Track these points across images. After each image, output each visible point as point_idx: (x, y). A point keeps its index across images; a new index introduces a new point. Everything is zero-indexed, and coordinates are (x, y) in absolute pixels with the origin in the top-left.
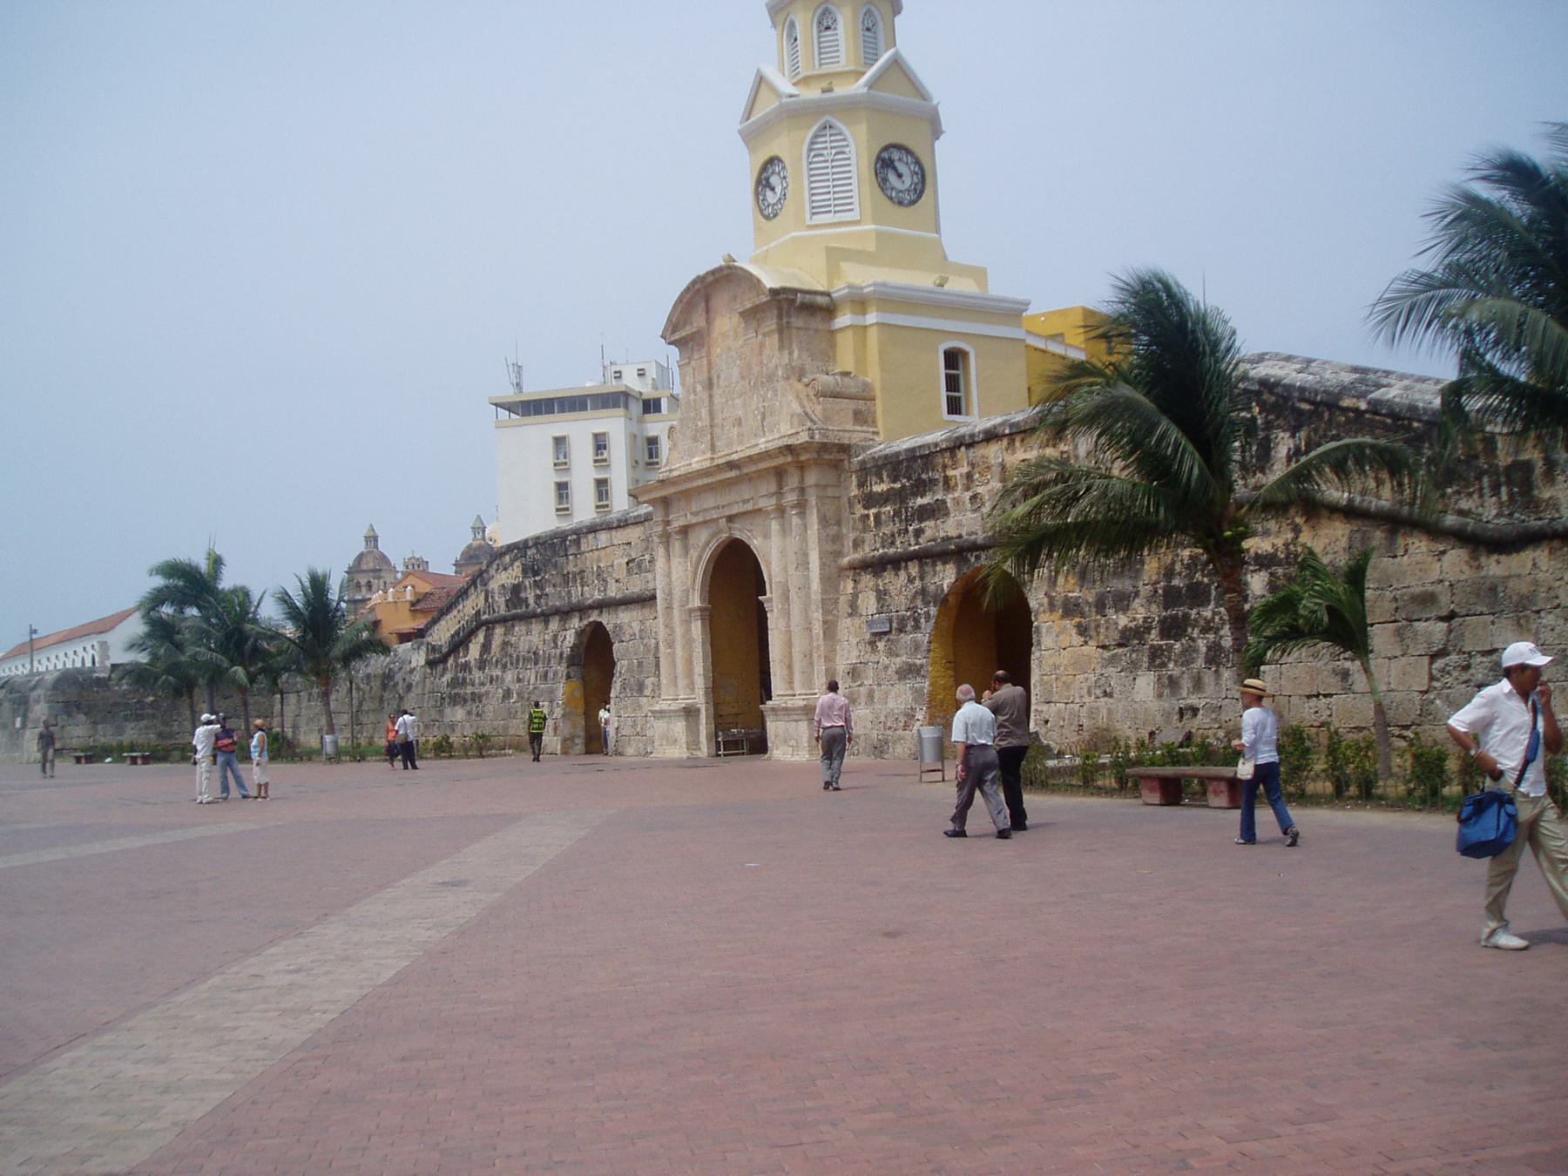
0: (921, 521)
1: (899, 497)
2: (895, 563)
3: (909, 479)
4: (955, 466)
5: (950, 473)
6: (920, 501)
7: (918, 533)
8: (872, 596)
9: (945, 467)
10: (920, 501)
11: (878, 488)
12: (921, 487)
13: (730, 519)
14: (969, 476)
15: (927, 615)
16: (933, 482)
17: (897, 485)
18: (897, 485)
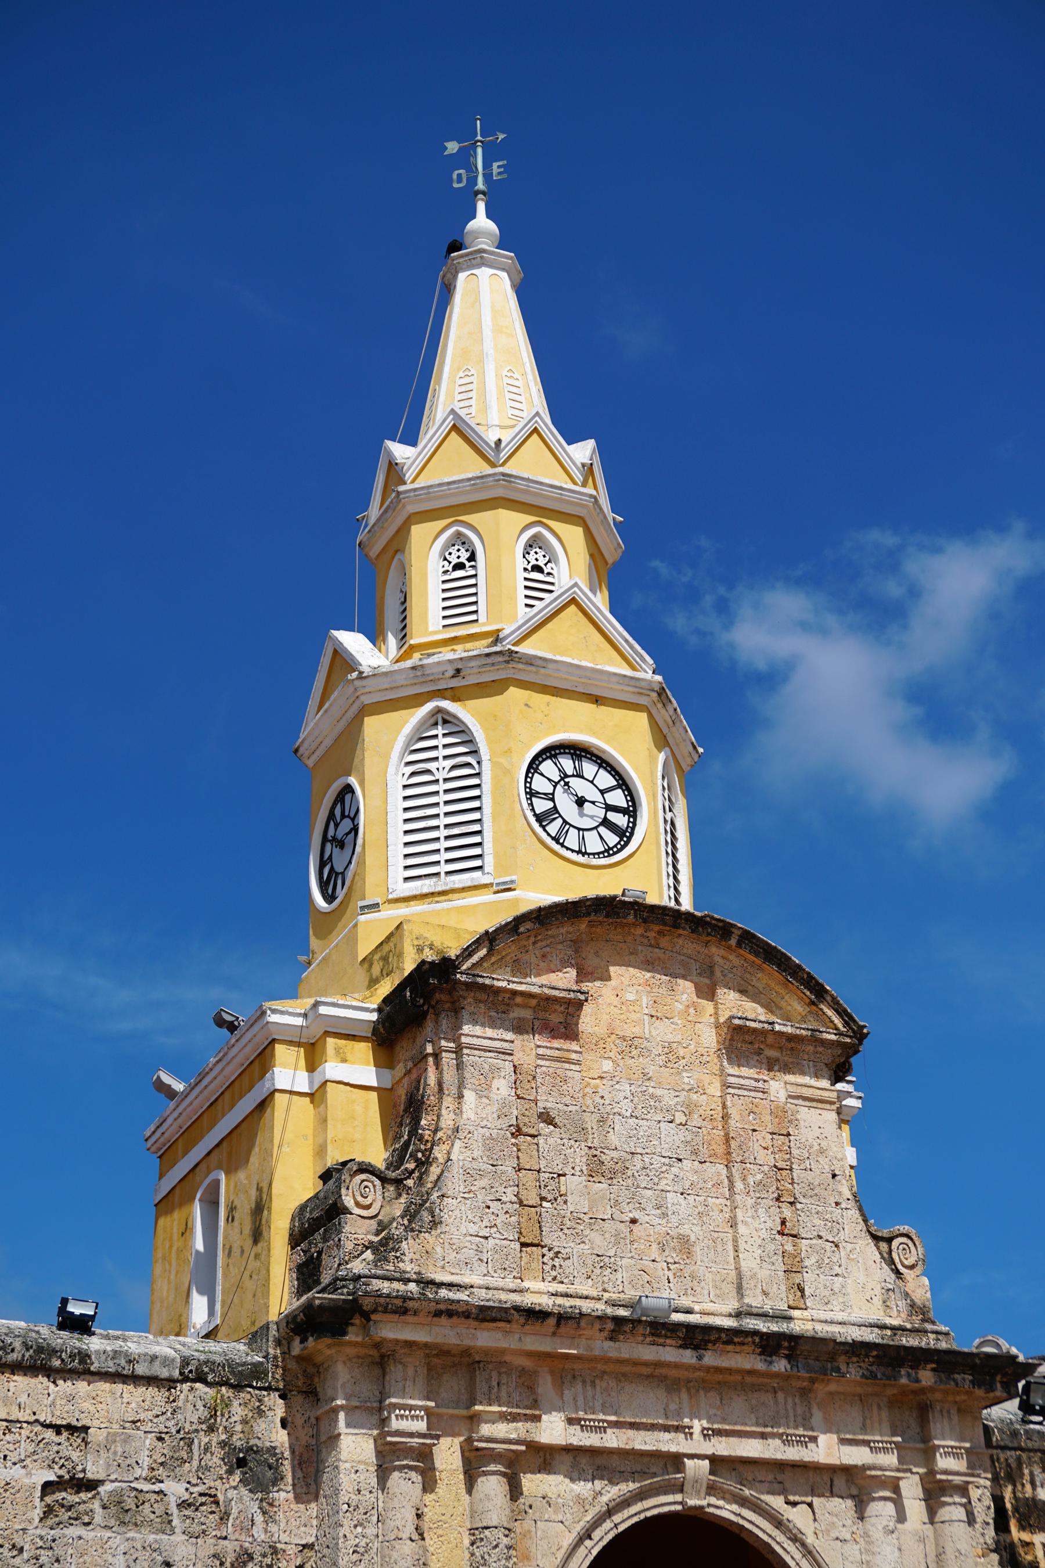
13: (717, 1462)
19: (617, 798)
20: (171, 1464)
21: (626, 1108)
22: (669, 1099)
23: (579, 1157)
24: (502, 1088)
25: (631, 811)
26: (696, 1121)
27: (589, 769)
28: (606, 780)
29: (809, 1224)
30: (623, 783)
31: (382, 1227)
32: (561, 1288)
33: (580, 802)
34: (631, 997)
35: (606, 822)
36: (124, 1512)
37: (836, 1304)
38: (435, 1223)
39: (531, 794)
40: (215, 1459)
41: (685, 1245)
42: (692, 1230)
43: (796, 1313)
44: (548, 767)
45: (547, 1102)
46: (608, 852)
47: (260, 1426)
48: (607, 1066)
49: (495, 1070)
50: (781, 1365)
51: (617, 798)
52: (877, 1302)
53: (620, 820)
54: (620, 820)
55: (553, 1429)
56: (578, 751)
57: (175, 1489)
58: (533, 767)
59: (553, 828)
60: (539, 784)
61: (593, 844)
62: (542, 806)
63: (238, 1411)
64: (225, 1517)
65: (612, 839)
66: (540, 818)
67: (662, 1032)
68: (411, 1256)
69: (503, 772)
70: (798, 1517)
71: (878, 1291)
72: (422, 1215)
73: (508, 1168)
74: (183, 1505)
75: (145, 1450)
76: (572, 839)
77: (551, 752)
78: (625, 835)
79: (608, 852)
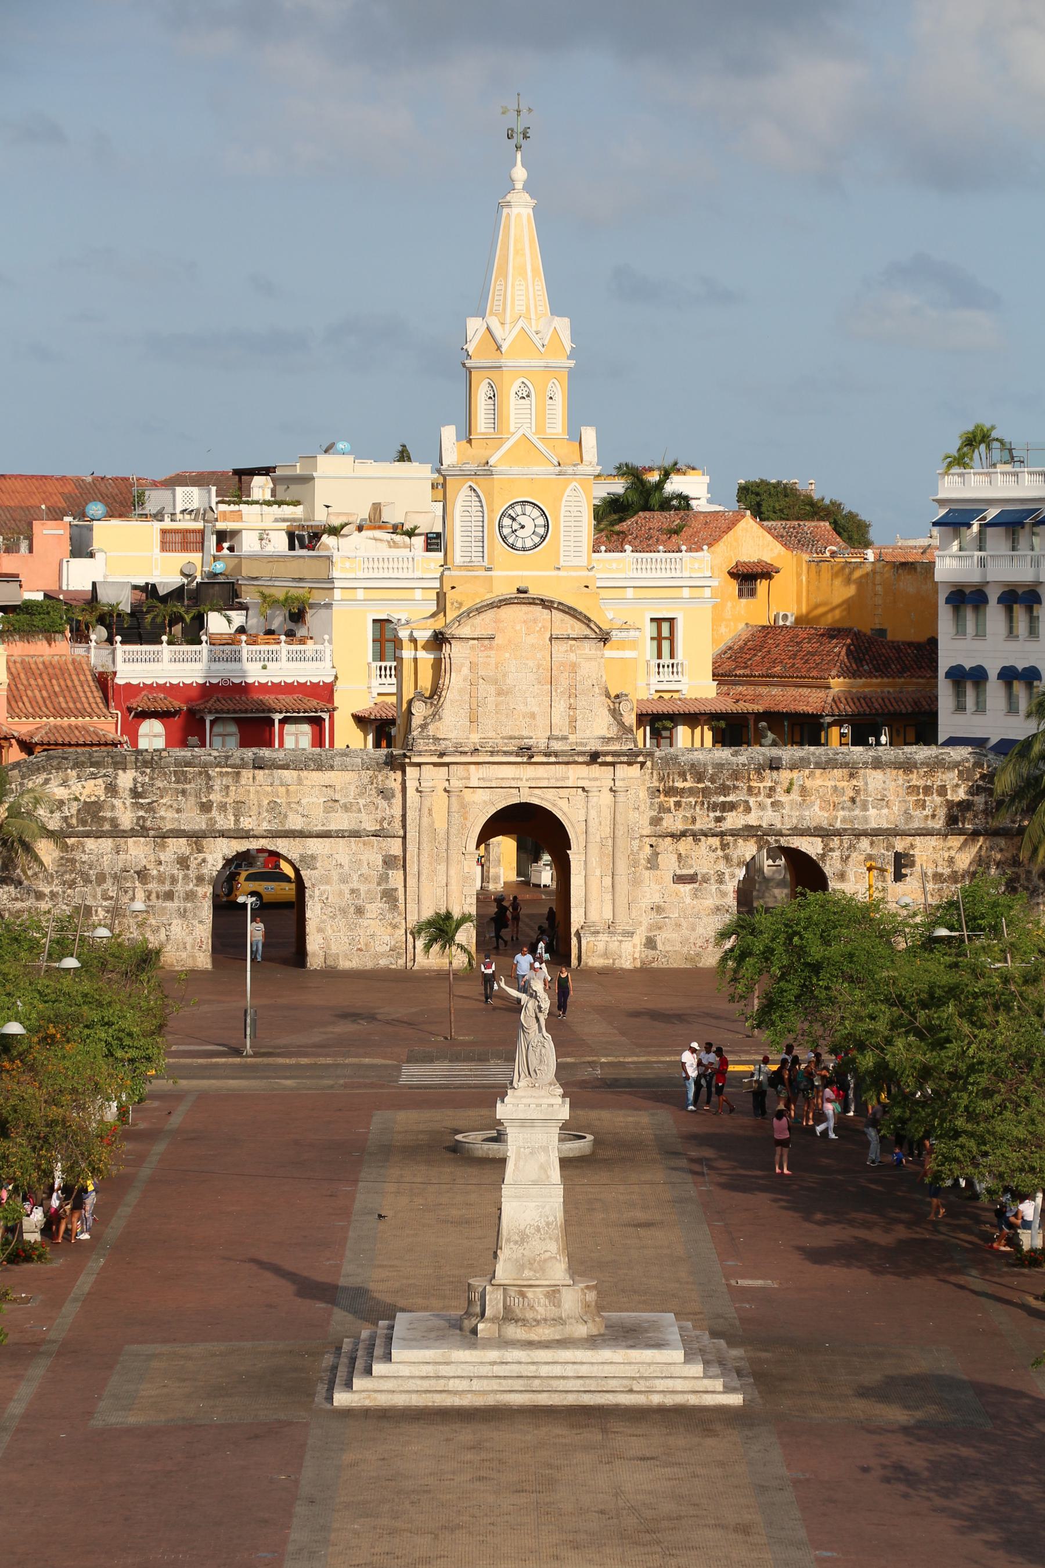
0: (723, 810)
1: (705, 792)
2: (696, 836)
3: (713, 782)
4: (762, 780)
5: (753, 784)
6: (722, 799)
7: (719, 820)
8: (674, 858)
9: (749, 779)
10: (722, 799)
11: (679, 784)
12: (724, 790)
14: (772, 789)
15: (733, 876)
16: (736, 788)
17: (700, 786)
18: (700, 786)
20: (361, 794)
21: (513, 669)
22: (531, 663)
23: (492, 689)
24: (465, 670)
26: (541, 670)
27: (529, 509)
28: (536, 513)
29: (581, 703)
31: (425, 718)
32: (483, 736)
33: (523, 527)
34: (518, 628)
36: (347, 808)
37: (588, 732)
38: (440, 719)
40: (373, 792)
41: (533, 716)
42: (536, 709)
43: (570, 736)
45: (481, 673)
47: (387, 782)
48: (507, 655)
49: (462, 665)
50: (553, 759)
52: (605, 729)
55: (474, 783)
57: (362, 802)
61: (529, 544)
63: (380, 778)
64: (377, 809)
67: (532, 639)
68: (431, 730)
69: (491, 520)
70: (563, 804)
71: (606, 726)
72: (435, 715)
73: (467, 697)
74: (364, 806)
75: (353, 790)
77: (512, 506)
78: (543, 538)
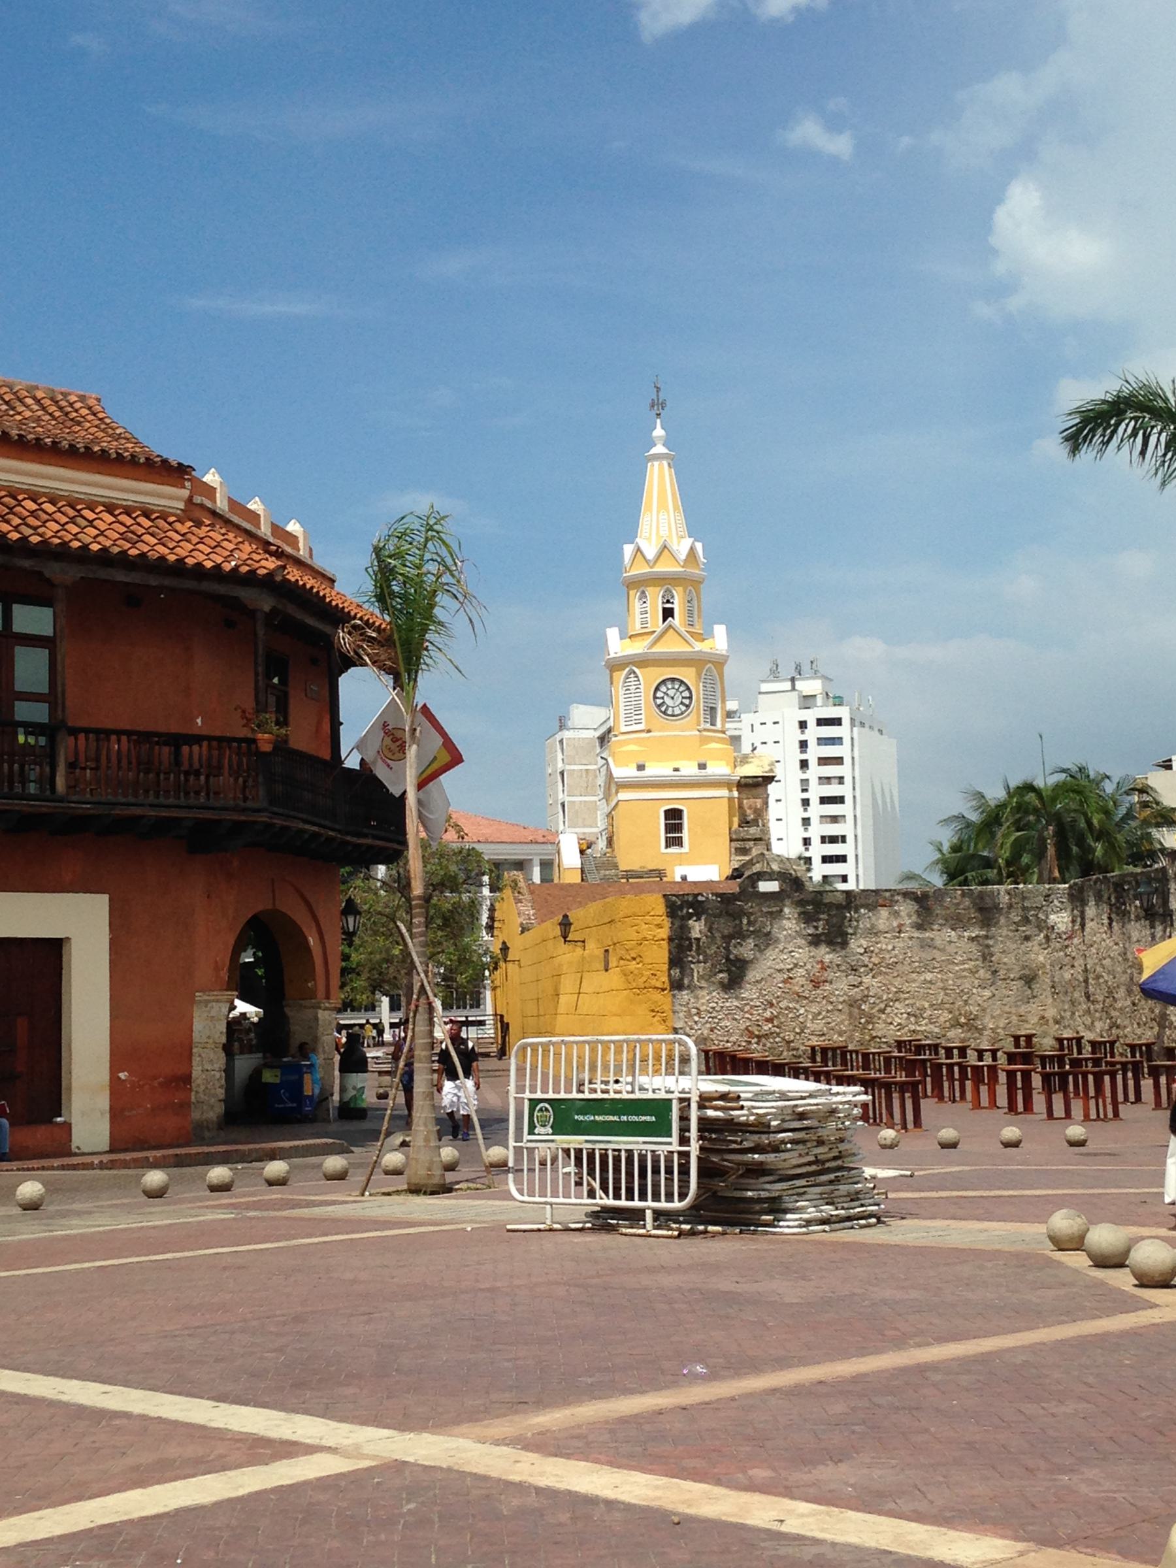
19: (686, 694)
25: (690, 698)
30: (688, 688)
35: (682, 703)
39: (655, 698)
44: (663, 689)
46: (682, 713)
51: (686, 694)
53: (687, 702)
54: (687, 702)
56: (673, 680)
58: (657, 689)
59: (663, 709)
60: (659, 694)
62: (659, 701)
65: (683, 708)
66: (659, 706)
69: (647, 695)
76: (669, 712)
77: (664, 682)
78: (688, 706)
79: (682, 713)
